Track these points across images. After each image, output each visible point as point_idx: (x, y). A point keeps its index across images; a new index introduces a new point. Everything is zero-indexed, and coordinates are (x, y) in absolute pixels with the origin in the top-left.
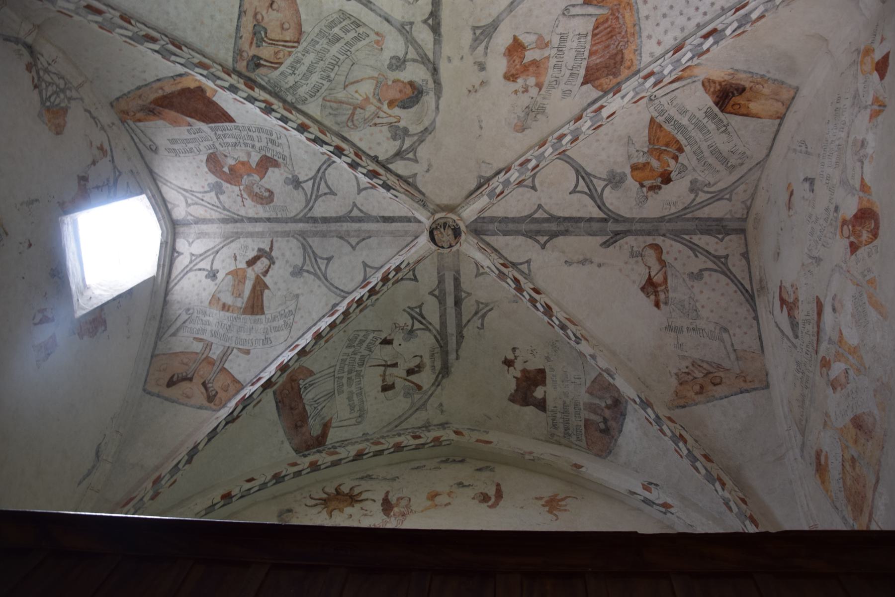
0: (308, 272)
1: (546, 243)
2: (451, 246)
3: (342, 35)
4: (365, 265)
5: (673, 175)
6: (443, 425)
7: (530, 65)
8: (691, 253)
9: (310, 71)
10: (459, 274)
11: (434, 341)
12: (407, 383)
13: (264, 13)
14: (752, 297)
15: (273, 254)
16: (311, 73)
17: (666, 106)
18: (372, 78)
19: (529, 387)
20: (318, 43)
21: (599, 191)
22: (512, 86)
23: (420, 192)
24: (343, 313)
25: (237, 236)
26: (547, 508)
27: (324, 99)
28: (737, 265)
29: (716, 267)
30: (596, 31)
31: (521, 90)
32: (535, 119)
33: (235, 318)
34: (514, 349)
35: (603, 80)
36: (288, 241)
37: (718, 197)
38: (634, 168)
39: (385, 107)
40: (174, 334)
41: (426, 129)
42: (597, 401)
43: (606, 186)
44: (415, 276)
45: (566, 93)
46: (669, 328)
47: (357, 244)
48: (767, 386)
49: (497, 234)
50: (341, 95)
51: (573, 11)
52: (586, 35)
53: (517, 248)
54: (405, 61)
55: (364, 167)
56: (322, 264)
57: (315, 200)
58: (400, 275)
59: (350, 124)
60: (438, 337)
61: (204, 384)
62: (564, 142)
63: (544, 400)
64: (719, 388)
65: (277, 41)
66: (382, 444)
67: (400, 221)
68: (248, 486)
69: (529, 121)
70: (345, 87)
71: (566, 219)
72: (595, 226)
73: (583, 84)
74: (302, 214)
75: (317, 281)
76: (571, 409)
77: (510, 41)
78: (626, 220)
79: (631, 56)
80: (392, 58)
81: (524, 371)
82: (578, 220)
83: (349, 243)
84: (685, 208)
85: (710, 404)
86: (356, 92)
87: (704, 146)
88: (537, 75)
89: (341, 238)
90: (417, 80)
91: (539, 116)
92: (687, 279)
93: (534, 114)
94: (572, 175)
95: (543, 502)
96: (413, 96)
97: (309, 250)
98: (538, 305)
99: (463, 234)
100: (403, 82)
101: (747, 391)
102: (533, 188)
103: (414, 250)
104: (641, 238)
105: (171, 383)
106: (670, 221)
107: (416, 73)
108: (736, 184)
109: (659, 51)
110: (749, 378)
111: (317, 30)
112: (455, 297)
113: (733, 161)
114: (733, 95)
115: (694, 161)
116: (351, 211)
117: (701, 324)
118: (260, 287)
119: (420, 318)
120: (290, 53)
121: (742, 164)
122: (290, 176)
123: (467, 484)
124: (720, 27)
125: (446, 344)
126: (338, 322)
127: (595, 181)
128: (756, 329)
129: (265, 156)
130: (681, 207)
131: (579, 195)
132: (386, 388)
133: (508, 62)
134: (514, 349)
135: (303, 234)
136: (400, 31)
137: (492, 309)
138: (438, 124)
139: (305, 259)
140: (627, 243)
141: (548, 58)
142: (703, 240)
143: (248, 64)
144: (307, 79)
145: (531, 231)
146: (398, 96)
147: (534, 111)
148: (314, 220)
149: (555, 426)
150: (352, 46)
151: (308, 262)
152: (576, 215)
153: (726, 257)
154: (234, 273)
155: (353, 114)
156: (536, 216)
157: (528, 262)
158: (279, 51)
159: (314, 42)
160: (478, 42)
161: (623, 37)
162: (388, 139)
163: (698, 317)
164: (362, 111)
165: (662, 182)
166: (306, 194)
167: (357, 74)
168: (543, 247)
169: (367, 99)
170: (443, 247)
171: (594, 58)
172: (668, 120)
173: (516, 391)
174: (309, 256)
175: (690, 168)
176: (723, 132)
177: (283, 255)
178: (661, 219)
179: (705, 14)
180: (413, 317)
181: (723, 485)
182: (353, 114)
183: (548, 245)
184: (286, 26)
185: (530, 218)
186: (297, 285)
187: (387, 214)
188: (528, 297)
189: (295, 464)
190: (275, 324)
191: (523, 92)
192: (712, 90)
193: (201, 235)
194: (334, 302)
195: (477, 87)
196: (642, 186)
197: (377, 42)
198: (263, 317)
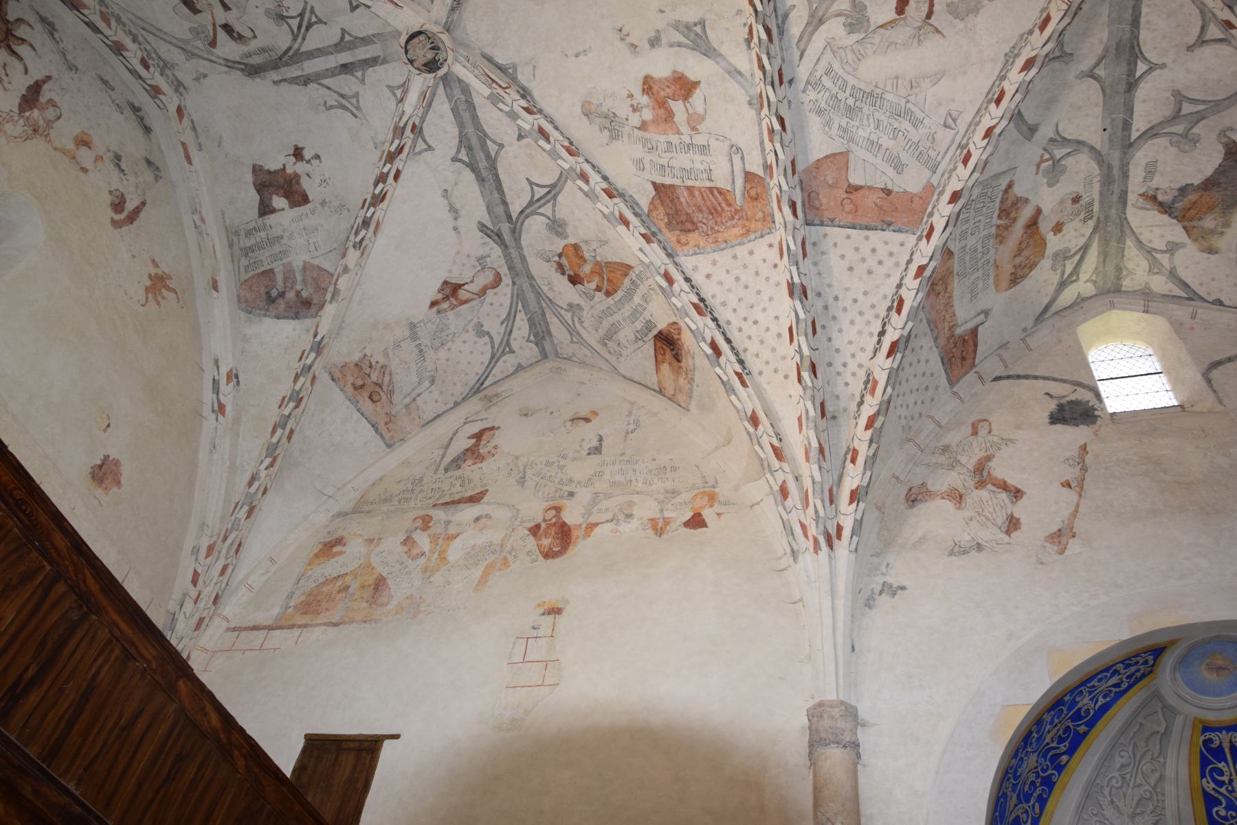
1: (460, 161)
5: (579, 286)
6: (179, 86)
7: (666, 109)
11: (284, 48)
12: (210, 28)
14: (478, 391)
19: (279, 187)
22: (637, 90)
26: (148, 283)
28: (507, 363)
31: (635, 102)
32: (603, 128)
35: (661, 210)
42: (299, 278)
46: (412, 326)
49: (450, 101)
51: (736, 159)
52: (710, 180)
60: (291, 53)
62: (580, 183)
63: (273, 211)
64: (369, 402)
66: (109, 26)
69: (598, 120)
71: (497, 176)
72: (500, 210)
73: (654, 184)
76: (277, 248)
77: (693, 78)
79: (692, 243)
81: (297, 177)
85: (348, 403)
87: (617, 317)
91: (606, 132)
92: (473, 323)
93: (608, 125)
94: (549, 180)
95: (153, 271)
98: (381, 186)
99: (432, 75)
101: (377, 430)
104: (503, 261)
106: (531, 285)
109: (698, 279)
110: (390, 425)
112: (351, 63)
113: (610, 344)
115: (600, 307)
119: (305, 24)
123: (123, 166)
124: (722, 360)
125: (287, 64)
128: (445, 408)
130: (550, 295)
134: (317, 157)
137: (356, 116)
141: (679, 133)
142: (522, 326)
145: (468, 140)
147: (611, 124)
149: (249, 233)
152: (504, 186)
153: (512, 351)
156: (489, 142)
157: (430, 148)
160: (686, 31)
168: (455, 159)
170: (406, 52)
171: (685, 193)
173: (269, 172)
175: (592, 303)
178: (531, 277)
179: (740, 330)
180: (301, 15)
181: (272, 465)
185: (484, 137)
188: (385, 170)
191: (632, 106)
195: (629, 40)
196: (560, 256)
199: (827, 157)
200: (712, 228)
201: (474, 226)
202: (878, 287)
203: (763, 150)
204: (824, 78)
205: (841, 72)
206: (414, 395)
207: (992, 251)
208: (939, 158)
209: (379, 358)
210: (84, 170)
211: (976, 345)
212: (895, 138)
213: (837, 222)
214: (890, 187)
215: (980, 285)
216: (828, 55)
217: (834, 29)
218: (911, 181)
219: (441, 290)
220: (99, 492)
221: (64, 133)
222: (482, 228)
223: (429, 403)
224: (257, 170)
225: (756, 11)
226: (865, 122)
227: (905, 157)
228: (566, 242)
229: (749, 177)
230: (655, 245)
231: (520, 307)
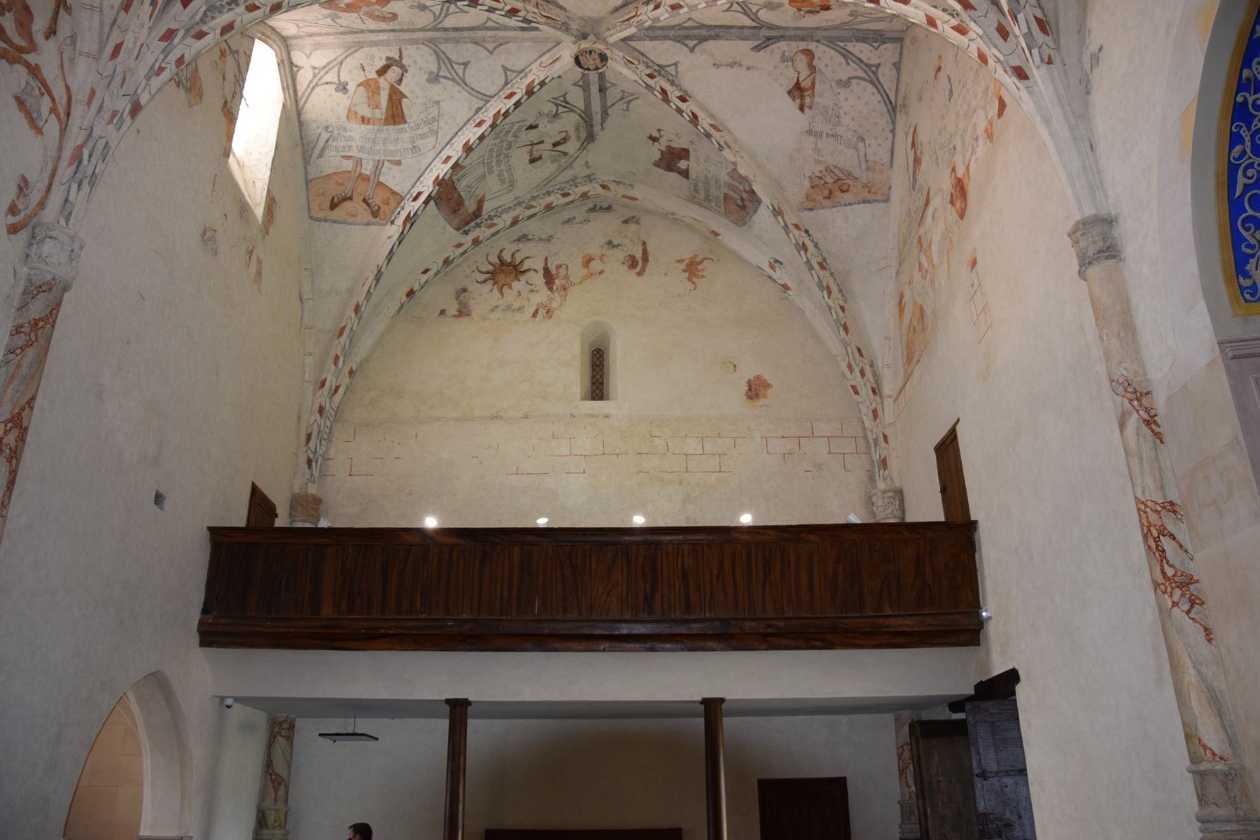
0: (445, 77)
1: (695, 46)
4: (505, 69)
6: (590, 178)
8: (843, 61)
14: (894, 109)
15: (404, 61)
25: (359, 46)
26: (687, 275)
29: (863, 75)
33: (379, 130)
34: (659, 130)
40: (321, 156)
46: (810, 132)
48: (887, 200)
53: (663, 52)
56: (460, 70)
61: (365, 201)
68: (424, 278)
71: (716, 27)
76: (713, 182)
78: (779, 28)
81: (668, 147)
92: (834, 86)
95: (683, 266)
101: (869, 202)
104: (794, 44)
105: (333, 206)
117: (840, 130)
118: (396, 97)
123: (615, 243)
125: (591, 119)
128: (890, 142)
132: (532, 161)
149: (696, 191)
152: (726, 23)
154: (366, 84)
157: (676, 64)
163: (839, 123)
168: (692, 50)
177: (415, 62)
178: (818, 28)
180: (557, 105)
181: (830, 293)
186: (436, 92)
189: (459, 245)
190: (419, 132)
193: (317, 47)
196: (799, 10)
198: (405, 125)
201: (753, 54)
206: (863, 159)
209: (818, 169)
210: (602, 272)
219: (794, 99)
220: (762, 401)
221: (576, 271)
222: (757, 49)
223: (877, 150)
224: (657, 164)
231: (842, 44)
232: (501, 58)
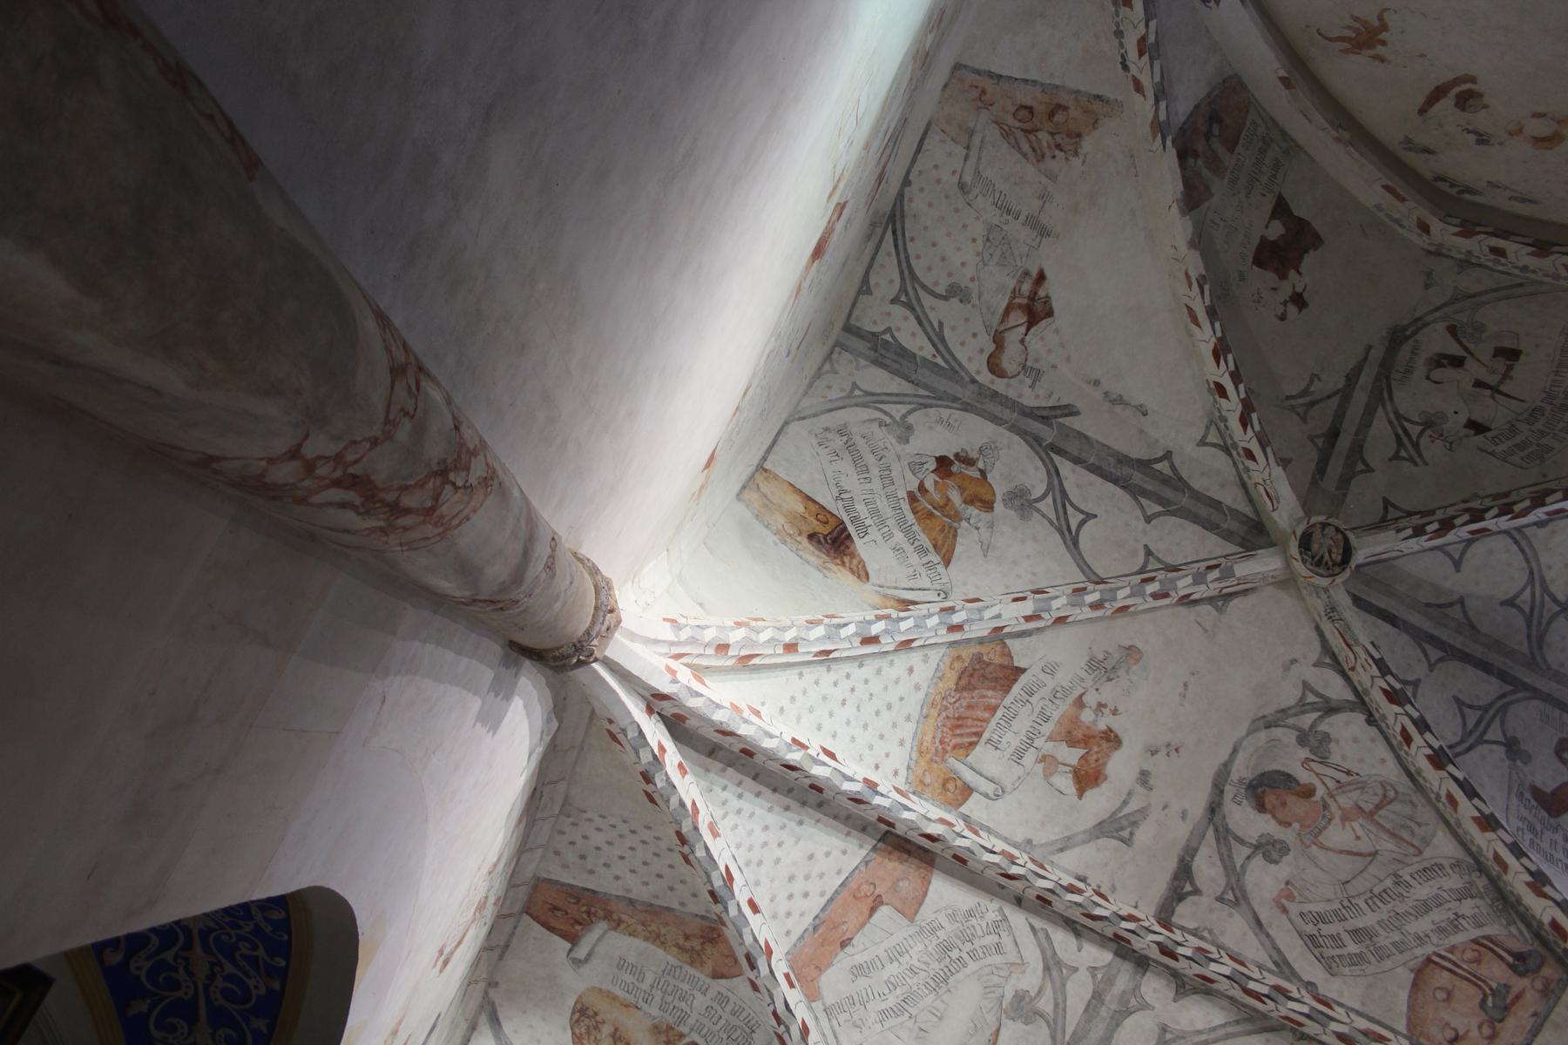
0: (1555, 600)
2: (1324, 525)
3: (1346, 937)
4: (1457, 564)
5: (932, 465)
6: (1437, 253)
8: (947, 332)
9: (1424, 908)
10: (1313, 477)
11: (1396, 394)
12: (1471, 346)
13: (1474, 1033)
16: (1425, 903)
17: (923, 571)
18: (1322, 847)
19: (1288, 247)
20: (1393, 944)
21: (1049, 499)
22: (1116, 723)
23: (1321, 634)
24: (1544, 505)
26: (1384, 36)
27: (1420, 852)
28: (887, 279)
29: (921, 293)
30: (974, 739)
34: (1283, 318)
35: (997, 660)
36: (1562, 665)
37: (873, 400)
38: (988, 506)
39: (1320, 792)
41: (1268, 727)
42: (1206, 172)
43: (1037, 500)
44: (1386, 509)
45: (1050, 669)
46: (1044, 232)
47: (1452, 604)
48: (957, 67)
50: (1387, 845)
51: (988, 787)
54: (1257, 847)
55: (1407, 714)
57: (1490, 705)
58: (1416, 520)
59: (1392, 794)
63: (1273, 216)
64: (1028, 101)
65: (1466, 979)
67: (1371, 605)
69: (1117, 656)
70: (1374, 854)
71: (1115, 481)
72: (1072, 447)
73: (1023, 671)
74: (1520, 695)
75: (1548, 579)
77: (1089, 794)
78: (1023, 433)
80: (1276, 862)
81: (1283, 276)
82: (1095, 470)
83: (1465, 612)
84: (926, 406)
85: (1057, 82)
86: (1358, 838)
87: (876, 485)
88: (1075, 721)
89: (1473, 627)
90: (1249, 809)
91: (1101, 657)
92: (975, 295)
95: (1380, 50)
96: (1267, 789)
97: (1534, 633)
99: (1299, 534)
100: (1274, 817)
101: (991, 75)
102: (1149, 553)
103: (1379, 549)
104: (1012, 394)
106: (955, 399)
107: (1248, 822)
108: (840, 404)
110: (975, 93)
111: (1388, 964)
112: (1333, 445)
113: (838, 442)
114: (825, 537)
115: (895, 473)
116: (1440, 660)
119: (1405, 440)
120: (1452, 949)
121: (826, 429)
122: (1519, 763)
123: (1472, 137)
125: (1377, 379)
126: (1559, 495)
127: (1053, 516)
129: (1550, 815)
130: (932, 411)
131: (1082, 507)
132: (1512, 354)
133: (1105, 764)
134: (1283, 318)
135: (1532, 663)
136: (1245, 897)
138: (1246, 724)
139: (1549, 623)
140: (1037, 397)
141: (1050, 739)
142: (918, 344)
143: (1539, 968)
144: (1437, 897)
145: (1176, 489)
146: (1292, 800)
148: (1503, 676)
149: (1277, 165)
150: (1335, 912)
151: (1547, 615)
152: (1099, 480)
153: (894, 301)
155: (1379, 807)
156: (1160, 509)
157: (1203, 443)
158: (1471, 962)
159: (1399, 947)
161: (946, 708)
162: (1337, 742)
164: (1362, 804)
165: (951, 463)
166: (1503, 723)
167: (1346, 866)
168: (1168, 455)
169: (1345, 819)
170: (1337, 530)
172: (921, 551)
173: (1306, 251)
174: (1540, 623)
176: (846, 492)
178: (967, 408)
180: (1416, 446)
182: (1379, 807)
183: (1161, 454)
184: (1441, 995)
185: (1171, 509)
187: (1387, 627)
191: (1105, 706)
192: (855, 561)
194: (1541, 532)
195: (1164, 752)
196: (983, 473)
197: (1290, 897)
199: (925, 894)
200: (946, 708)
201: (1079, 405)
202: (772, 881)
203: (998, 835)
204: (995, 938)
205: (989, 960)
206: (974, 153)
207: (655, 1012)
208: (834, 1022)
210: (1536, 115)
211: (551, 929)
212: (888, 982)
213: (862, 868)
214: (848, 950)
215: (628, 978)
216: (1012, 957)
217: (1030, 979)
218: (835, 981)
219: (1048, 298)
222: (1069, 410)
225: (1123, 918)
226: (926, 958)
227: (863, 982)
228: (999, 497)
229: (967, 791)
230: (985, 633)
231: (939, 361)
232: (1454, 583)
